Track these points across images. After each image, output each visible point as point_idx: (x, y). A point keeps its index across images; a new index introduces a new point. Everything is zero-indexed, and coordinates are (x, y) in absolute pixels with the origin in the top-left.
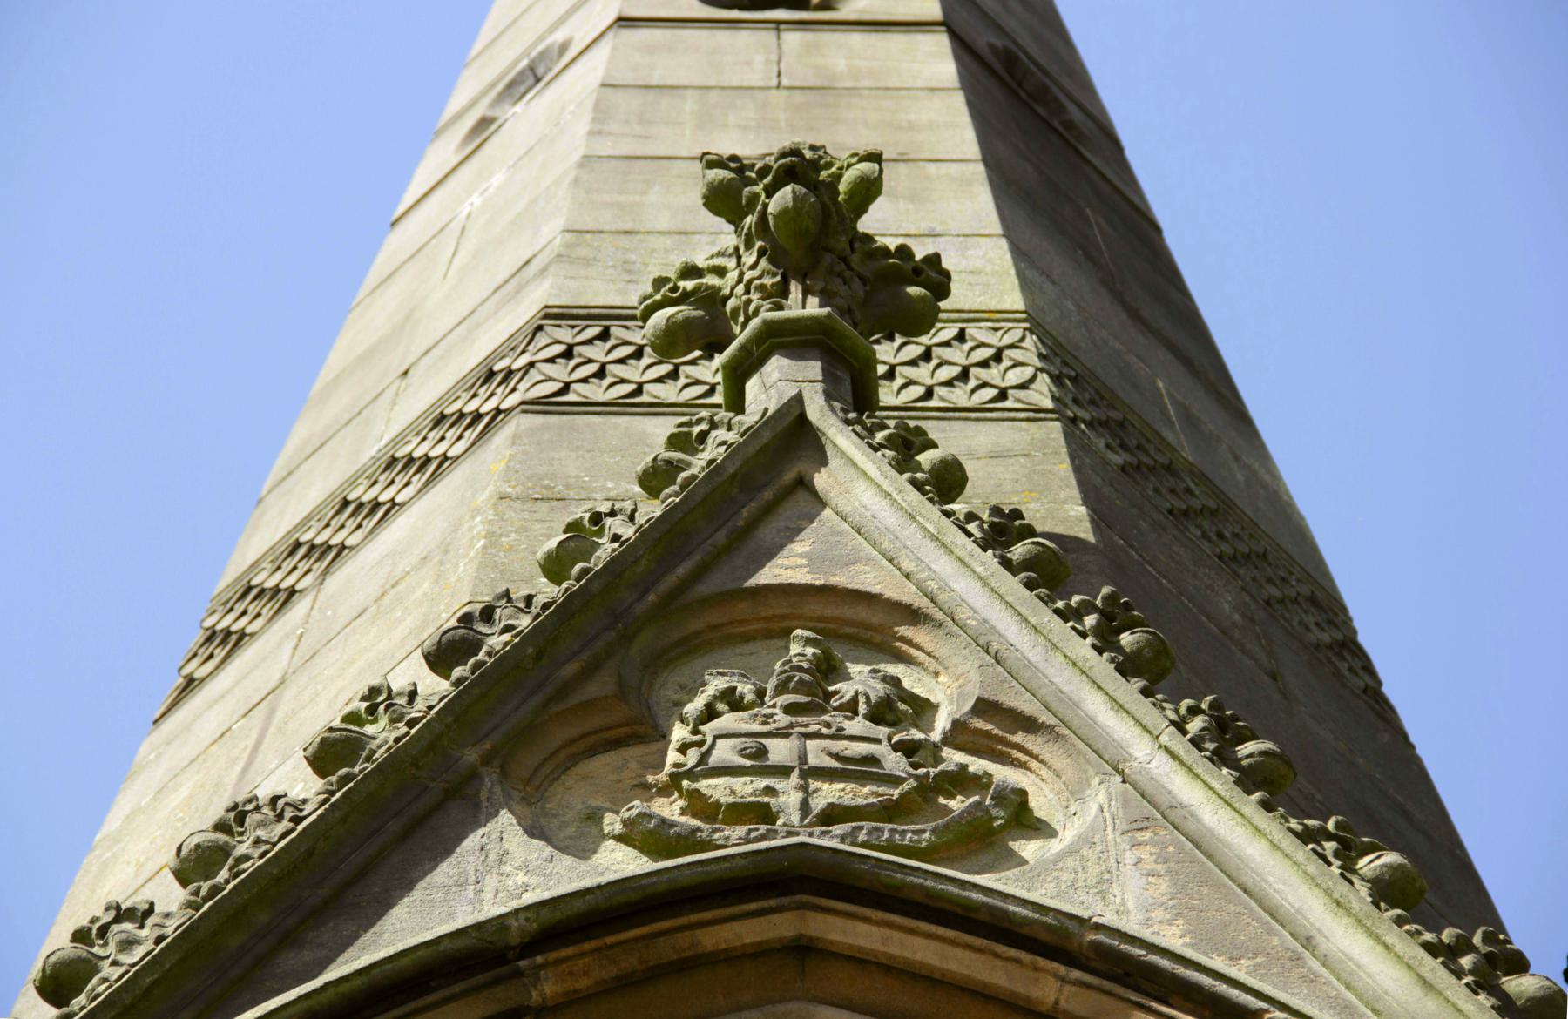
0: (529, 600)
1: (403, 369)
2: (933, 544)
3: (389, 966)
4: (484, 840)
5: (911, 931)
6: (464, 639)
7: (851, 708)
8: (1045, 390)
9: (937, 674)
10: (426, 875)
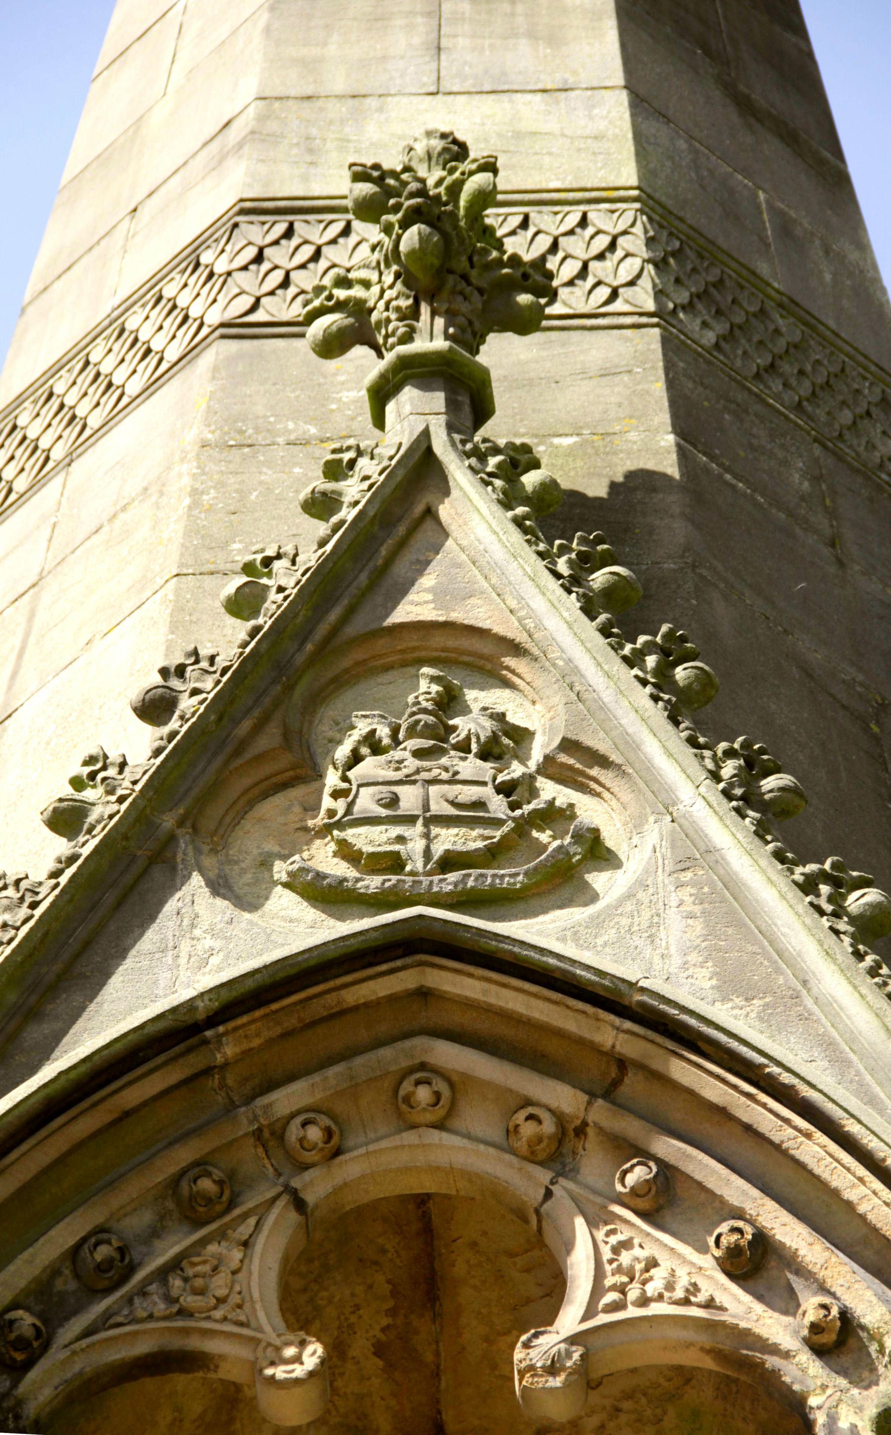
0: (212, 659)
1: (132, 207)
2: (531, 583)
3: (106, 1052)
4: (180, 904)
5: (505, 986)
6: (162, 698)
7: (464, 747)
8: (649, 287)
9: (534, 703)
10: (135, 942)
